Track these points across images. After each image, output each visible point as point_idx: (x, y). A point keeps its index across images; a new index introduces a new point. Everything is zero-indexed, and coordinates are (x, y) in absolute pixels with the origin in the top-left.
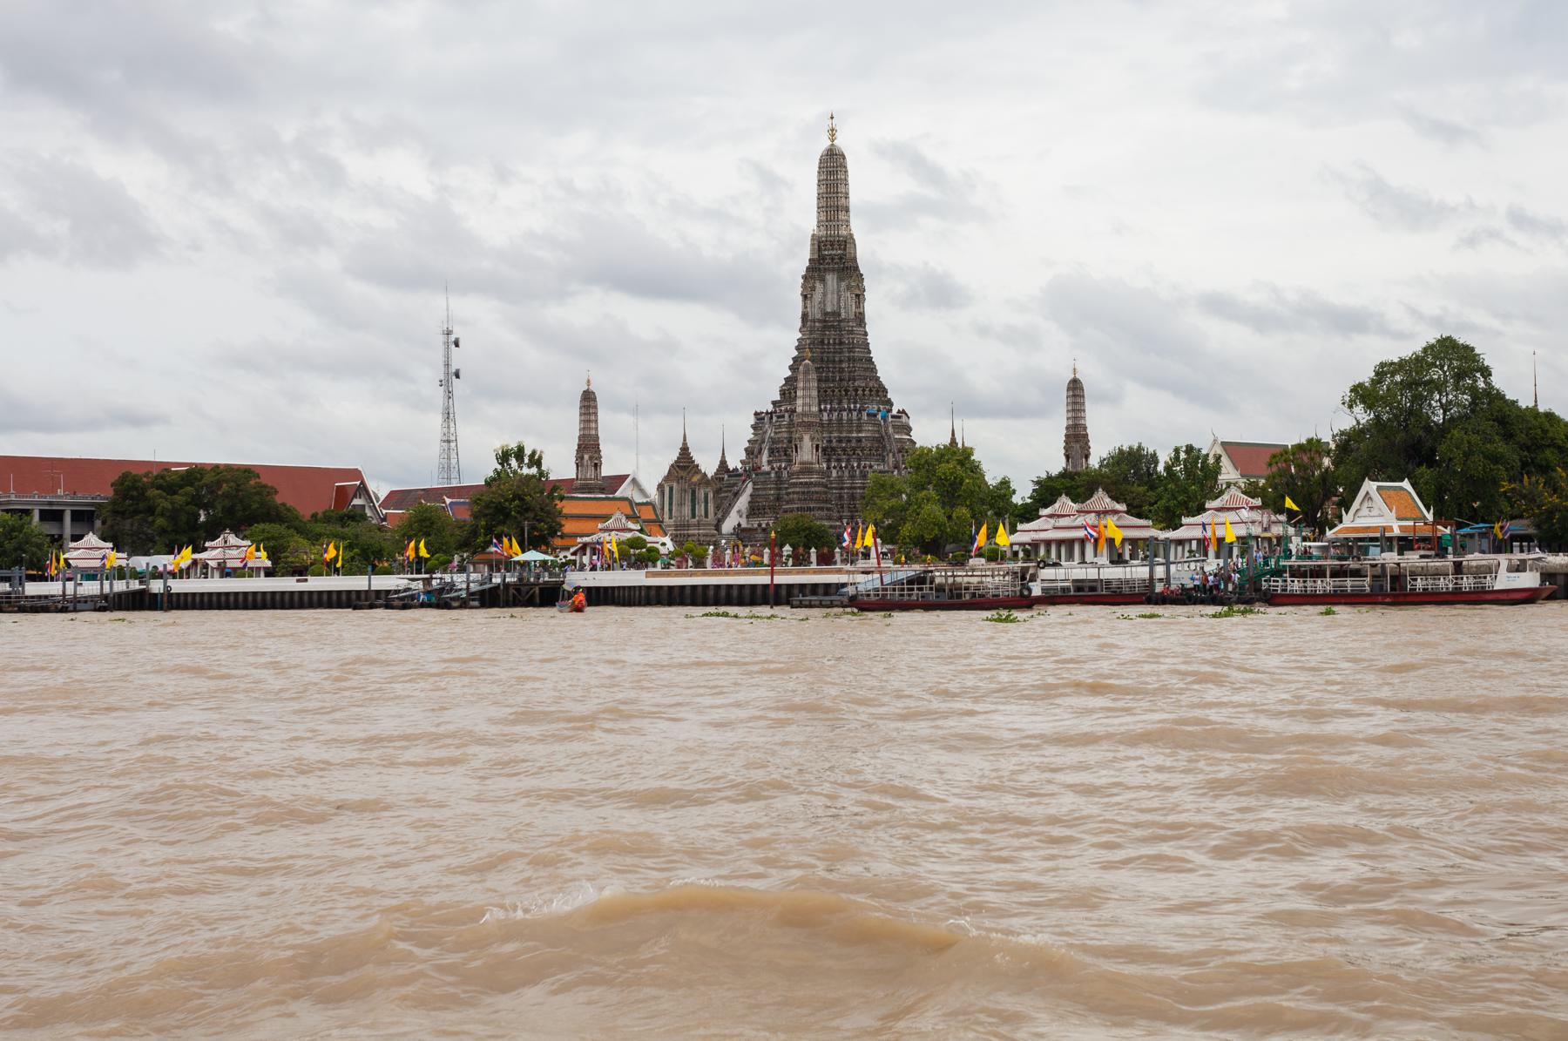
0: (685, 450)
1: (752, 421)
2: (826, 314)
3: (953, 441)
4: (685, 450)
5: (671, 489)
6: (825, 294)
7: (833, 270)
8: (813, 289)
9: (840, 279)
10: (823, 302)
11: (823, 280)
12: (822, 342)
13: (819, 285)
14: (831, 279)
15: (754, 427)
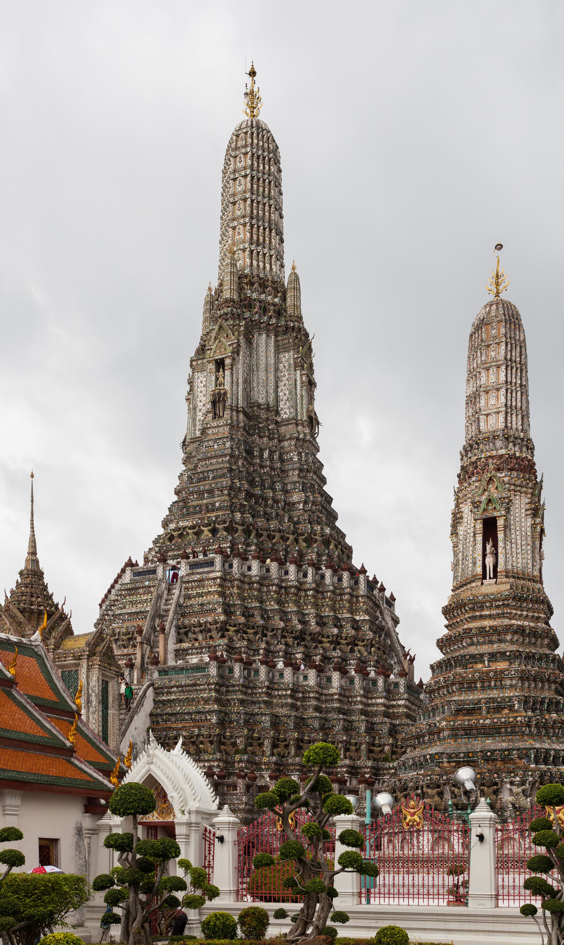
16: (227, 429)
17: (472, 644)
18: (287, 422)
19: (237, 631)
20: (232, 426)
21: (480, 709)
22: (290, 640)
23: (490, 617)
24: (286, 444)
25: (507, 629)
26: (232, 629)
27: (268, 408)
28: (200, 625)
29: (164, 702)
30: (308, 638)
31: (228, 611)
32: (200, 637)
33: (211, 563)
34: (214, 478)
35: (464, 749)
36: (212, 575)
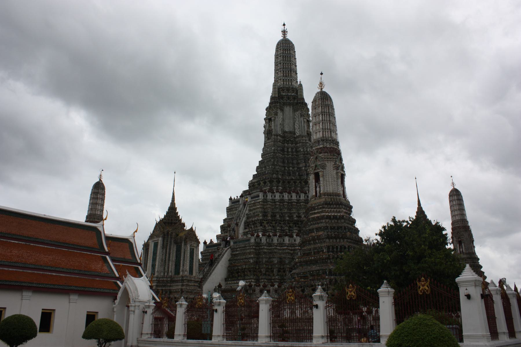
0: (172, 209)
1: (227, 204)
2: (284, 132)
3: (420, 212)
4: (172, 209)
5: (156, 245)
6: (283, 120)
7: (290, 104)
8: (276, 114)
9: (295, 111)
10: (282, 125)
11: (282, 110)
12: (283, 150)
13: (280, 113)
14: (288, 110)
15: (229, 210)
16: (272, 143)
17: (311, 225)
18: (298, 137)
19: (267, 223)
20: (274, 141)
21: (311, 252)
22: (291, 225)
23: (318, 213)
24: (298, 145)
25: (323, 217)
26: (265, 222)
27: (290, 132)
28: (253, 221)
29: (235, 255)
30: (300, 223)
31: (265, 215)
32: (253, 227)
33: (258, 196)
34: (267, 162)
35: (303, 271)
36: (258, 201)
